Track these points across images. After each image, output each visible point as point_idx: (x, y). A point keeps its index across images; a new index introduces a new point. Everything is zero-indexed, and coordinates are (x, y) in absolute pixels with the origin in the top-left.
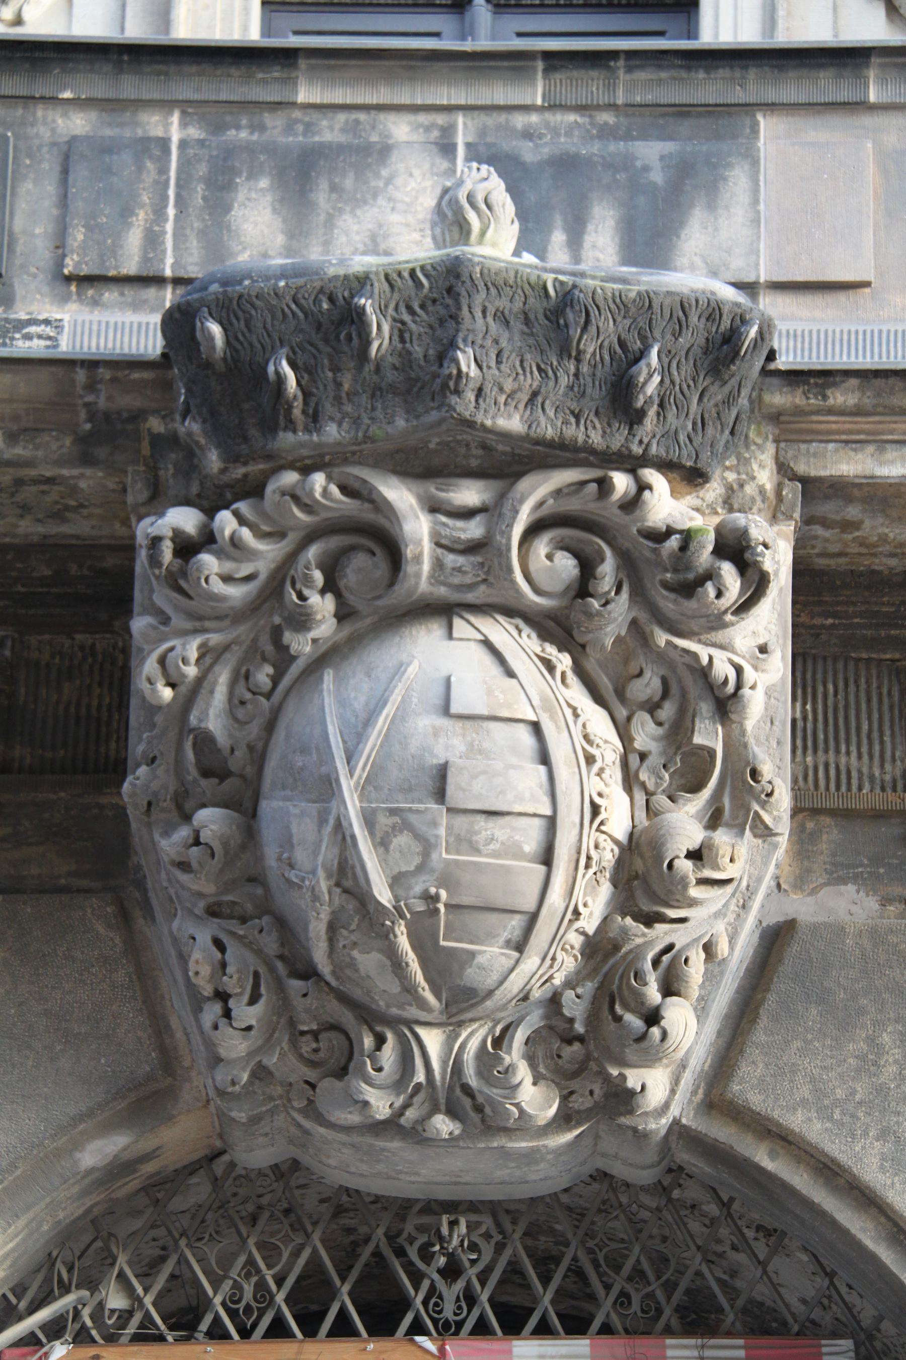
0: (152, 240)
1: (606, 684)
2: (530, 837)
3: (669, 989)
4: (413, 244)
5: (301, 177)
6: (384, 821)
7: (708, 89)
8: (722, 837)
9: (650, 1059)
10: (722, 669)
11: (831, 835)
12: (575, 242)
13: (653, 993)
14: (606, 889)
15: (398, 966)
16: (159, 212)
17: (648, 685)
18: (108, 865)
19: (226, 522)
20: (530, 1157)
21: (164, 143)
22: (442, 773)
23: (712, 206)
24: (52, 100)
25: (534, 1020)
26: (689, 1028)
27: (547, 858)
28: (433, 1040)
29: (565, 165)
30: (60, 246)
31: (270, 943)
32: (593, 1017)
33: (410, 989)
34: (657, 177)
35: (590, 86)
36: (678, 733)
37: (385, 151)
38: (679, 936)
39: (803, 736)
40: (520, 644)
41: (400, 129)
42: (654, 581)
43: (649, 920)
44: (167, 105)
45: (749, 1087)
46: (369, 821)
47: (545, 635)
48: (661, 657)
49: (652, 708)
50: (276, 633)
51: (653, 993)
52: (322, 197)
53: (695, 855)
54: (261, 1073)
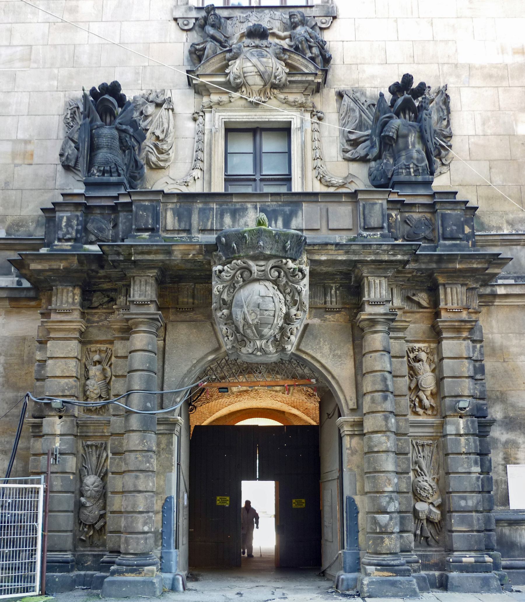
0: (212, 224)
1: (282, 290)
2: (272, 314)
3: (291, 334)
4: (252, 225)
5: (235, 214)
6: (251, 312)
7: (295, 199)
8: (299, 312)
9: (288, 344)
10: (299, 288)
11: (314, 311)
12: (276, 223)
13: (289, 334)
14: (282, 320)
15: (253, 333)
16: (213, 219)
17: (288, 290)
18: (210, 317)
19: (226, 267)
20: (271, 357)
21: (213, 208)
22: (259, 304)
23: (296, 217)
24: (196, 202)
25: (272, 339)
26: (294, 339)
27: (274, 316)
28: (258, 343)
29: (274, 211)
30: (199, 225)
31: (234, 329)
32: (281, 338)
33: (254, 335)
34: (288, 213)
35: (278, 198)
36: (293, 297)
37: (247, 209)
38: (293, 327)
39: (310, 297)
40: (269, 285)
41: (249, 205)
42: (289, 275)
43: (289, 324)
44: (213, 202)
45: (302, 347)
46: (248, 312)
47: (273, 284)
48: (290, 286)
49: (289, 294)
50: (234, 284)
51: (289, 334)
52: (237, 216)
53: (295, 315)
54: (233, 347)
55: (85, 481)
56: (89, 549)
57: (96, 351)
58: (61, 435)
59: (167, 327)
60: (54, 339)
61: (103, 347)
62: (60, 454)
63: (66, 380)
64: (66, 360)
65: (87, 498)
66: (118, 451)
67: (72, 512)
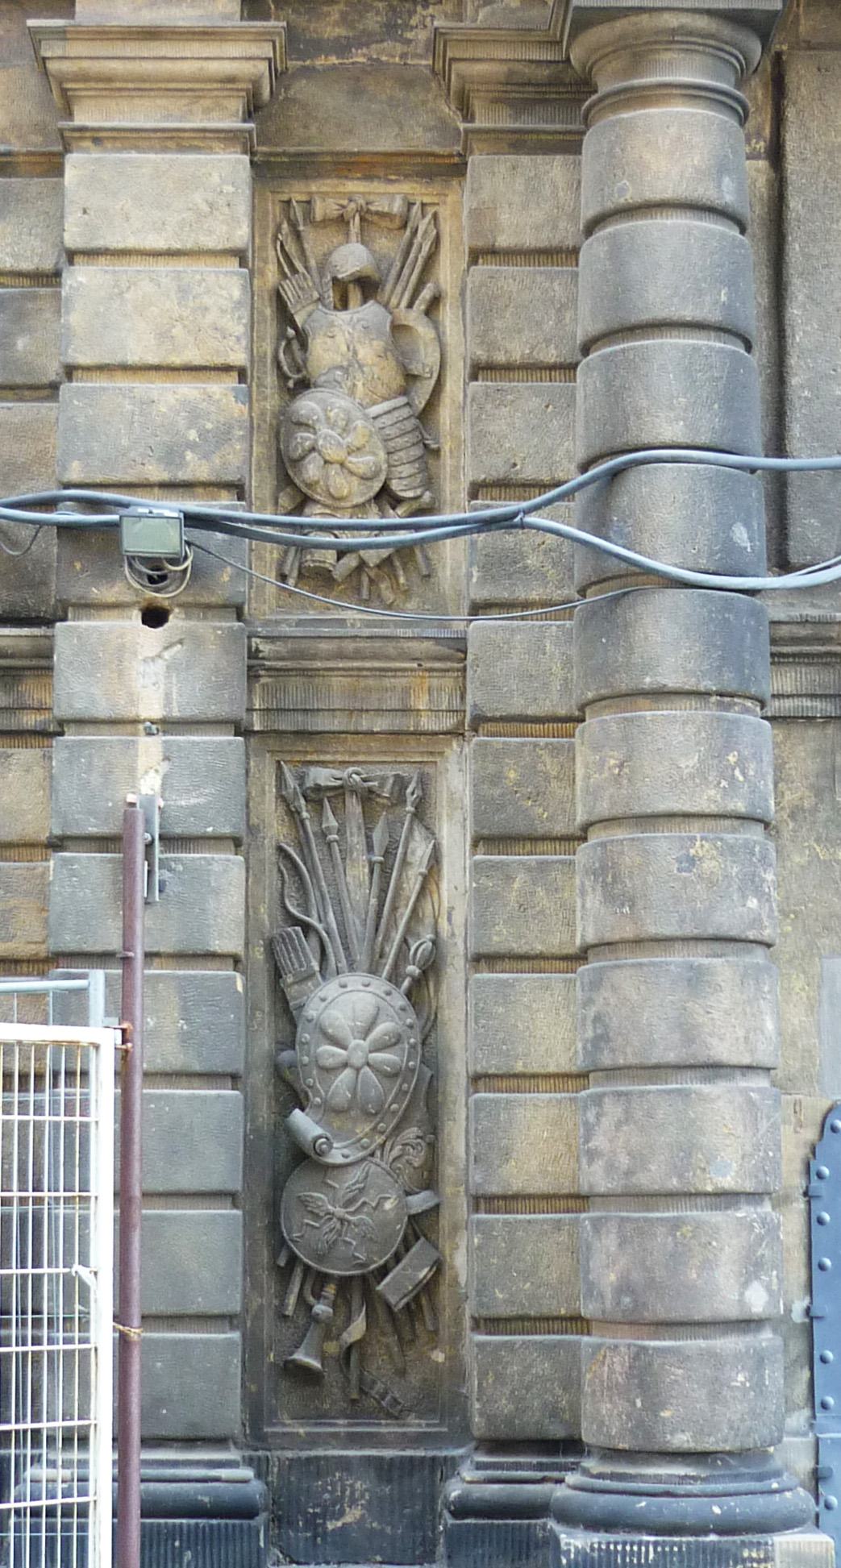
55: (311, 1011)
56: (342, 1426)
57: (342, 221)
58: (168, 725)
59: (791, 79)
60: (97, 137)
61: (389, 196)
62: (171, 841)
63: (188, 389)
64: (180, 265)
65: (330, 1111)
66: (521, 827)
67: (229, 1196)
